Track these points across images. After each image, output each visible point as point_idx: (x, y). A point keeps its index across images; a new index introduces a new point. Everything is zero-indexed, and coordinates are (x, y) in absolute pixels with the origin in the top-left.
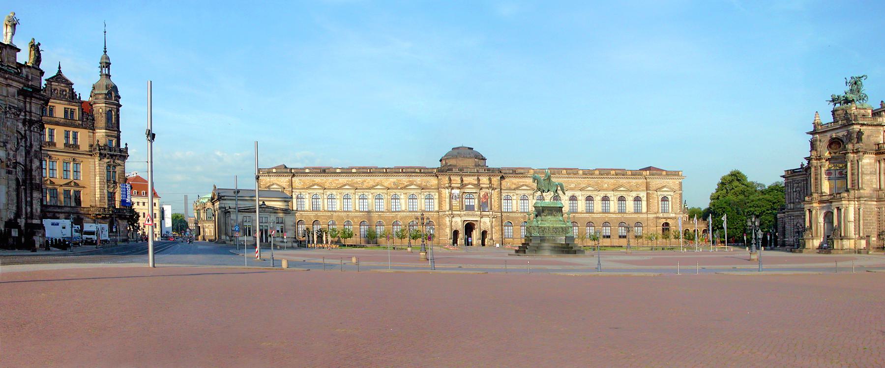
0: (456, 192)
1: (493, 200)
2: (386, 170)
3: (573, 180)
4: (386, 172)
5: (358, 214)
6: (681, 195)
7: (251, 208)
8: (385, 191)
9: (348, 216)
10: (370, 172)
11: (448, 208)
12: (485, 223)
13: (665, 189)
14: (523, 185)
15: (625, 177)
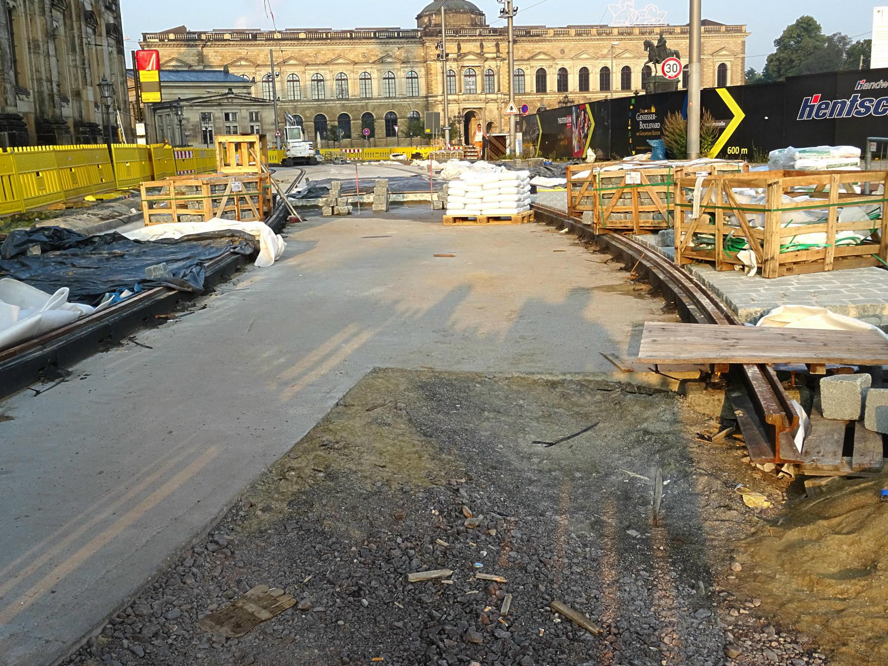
0: (452, 65)
1: (501, 76)
2: (351, 35)
3: (606, 43)
4: (351, 38)
5: (311, 104)
6: (743, 59)
7: (212, 98)
8: (350, 67)
9: (295, 108)
10: (327, 38)
11: (440, 92)
12: (491, 111)
13: (724, 52)
14: (539, 53)
15: (673, 36)
